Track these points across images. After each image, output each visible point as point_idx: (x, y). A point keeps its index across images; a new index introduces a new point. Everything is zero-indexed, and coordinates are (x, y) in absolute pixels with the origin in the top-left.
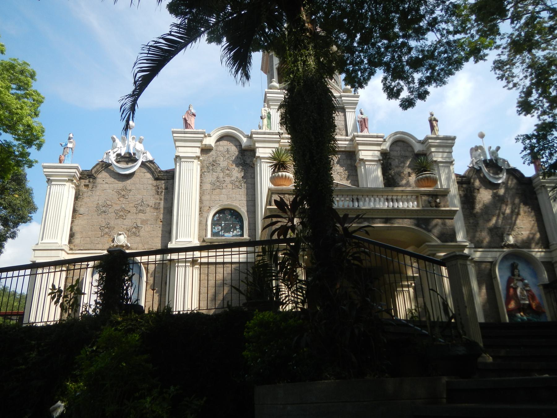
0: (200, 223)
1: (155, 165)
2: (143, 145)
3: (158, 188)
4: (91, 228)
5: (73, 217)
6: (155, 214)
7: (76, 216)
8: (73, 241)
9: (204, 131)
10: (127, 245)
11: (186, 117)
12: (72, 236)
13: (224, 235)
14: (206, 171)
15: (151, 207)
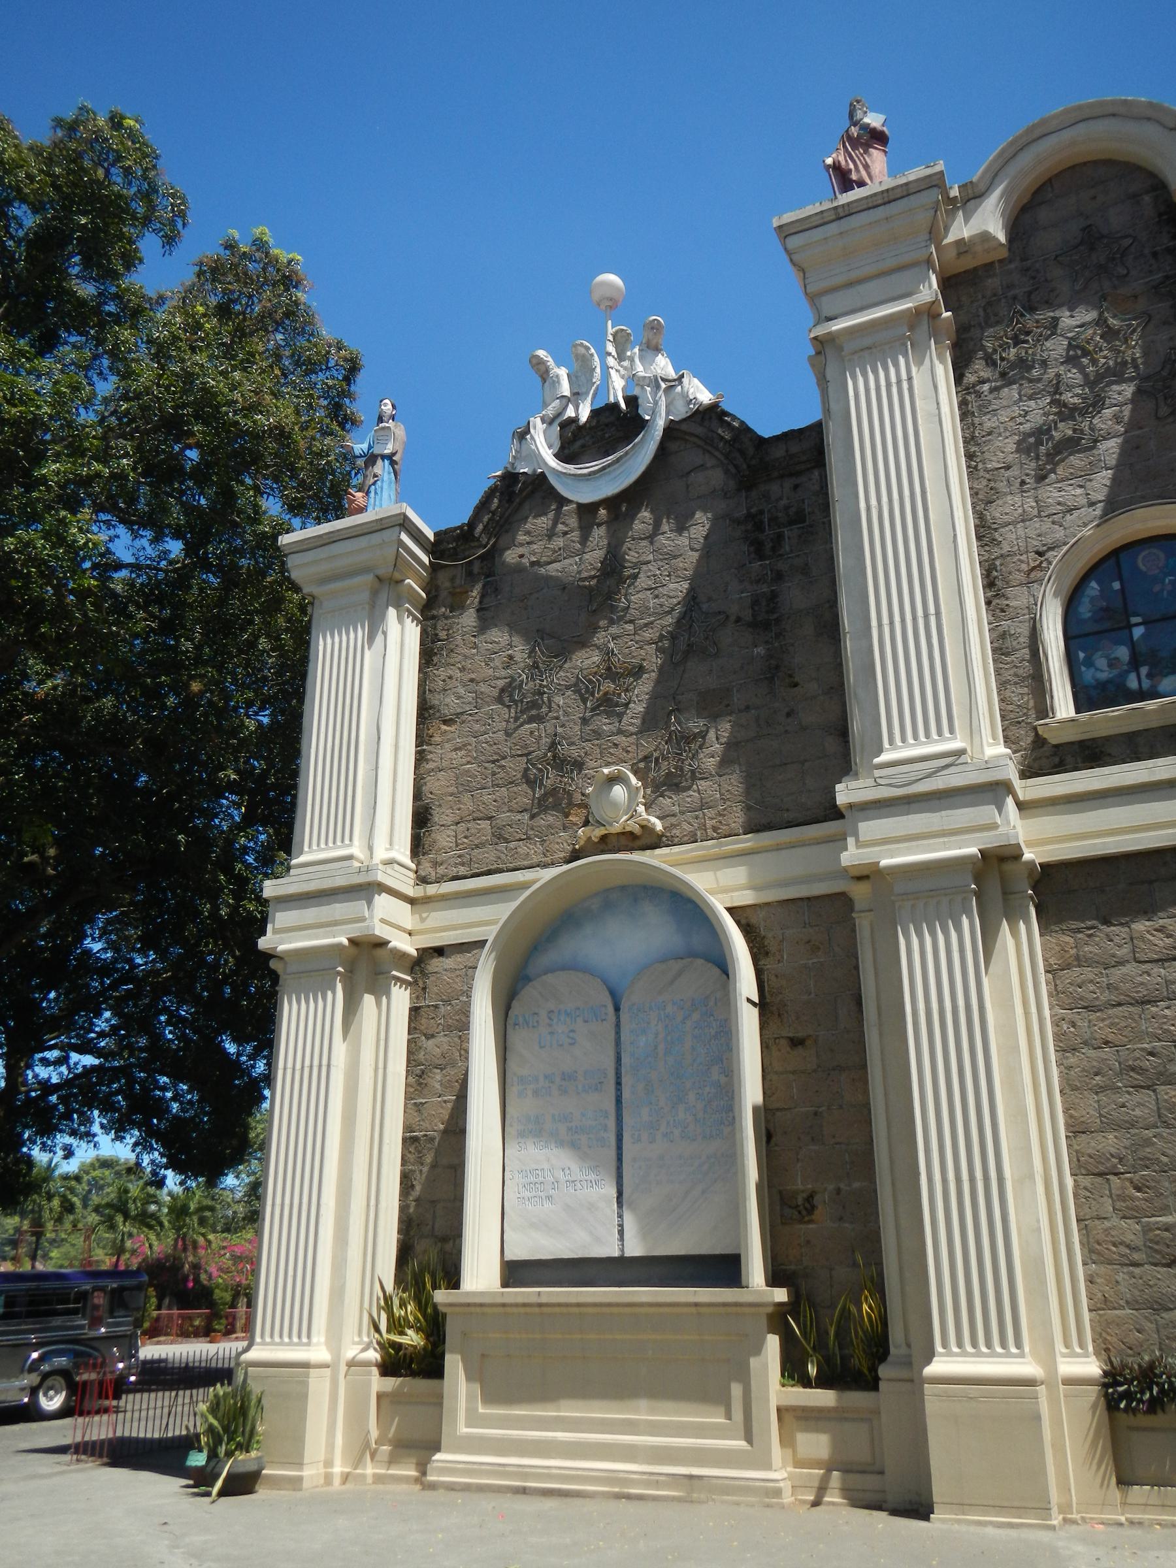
0: (1001, 649)
1: (729, 424)
2: (668, 356)
3: (759, 527)
4: (494, 774)
5: (422, 739)
6: (760, 650)
7: (430, 732)
8: (427, 841)
9: (940, 166)
10: (646, 828)
11: (841, 159)
12: (421, 819)
13: (1154, 686)
14: (985, 374)
15: (738, 620)
